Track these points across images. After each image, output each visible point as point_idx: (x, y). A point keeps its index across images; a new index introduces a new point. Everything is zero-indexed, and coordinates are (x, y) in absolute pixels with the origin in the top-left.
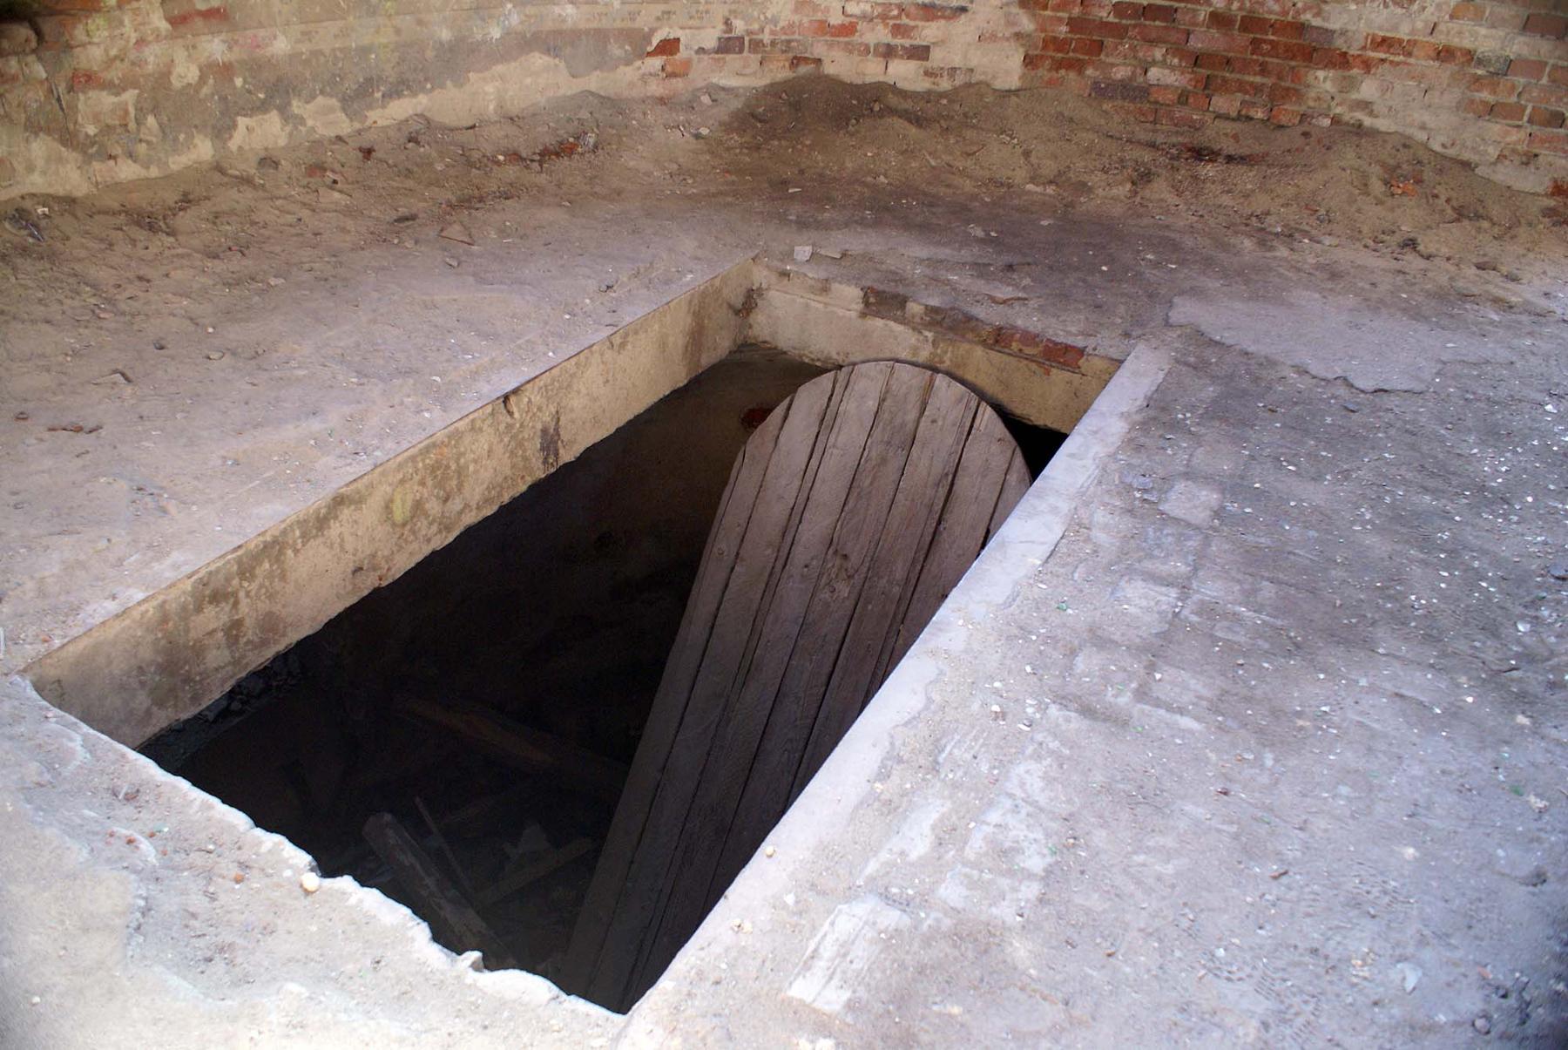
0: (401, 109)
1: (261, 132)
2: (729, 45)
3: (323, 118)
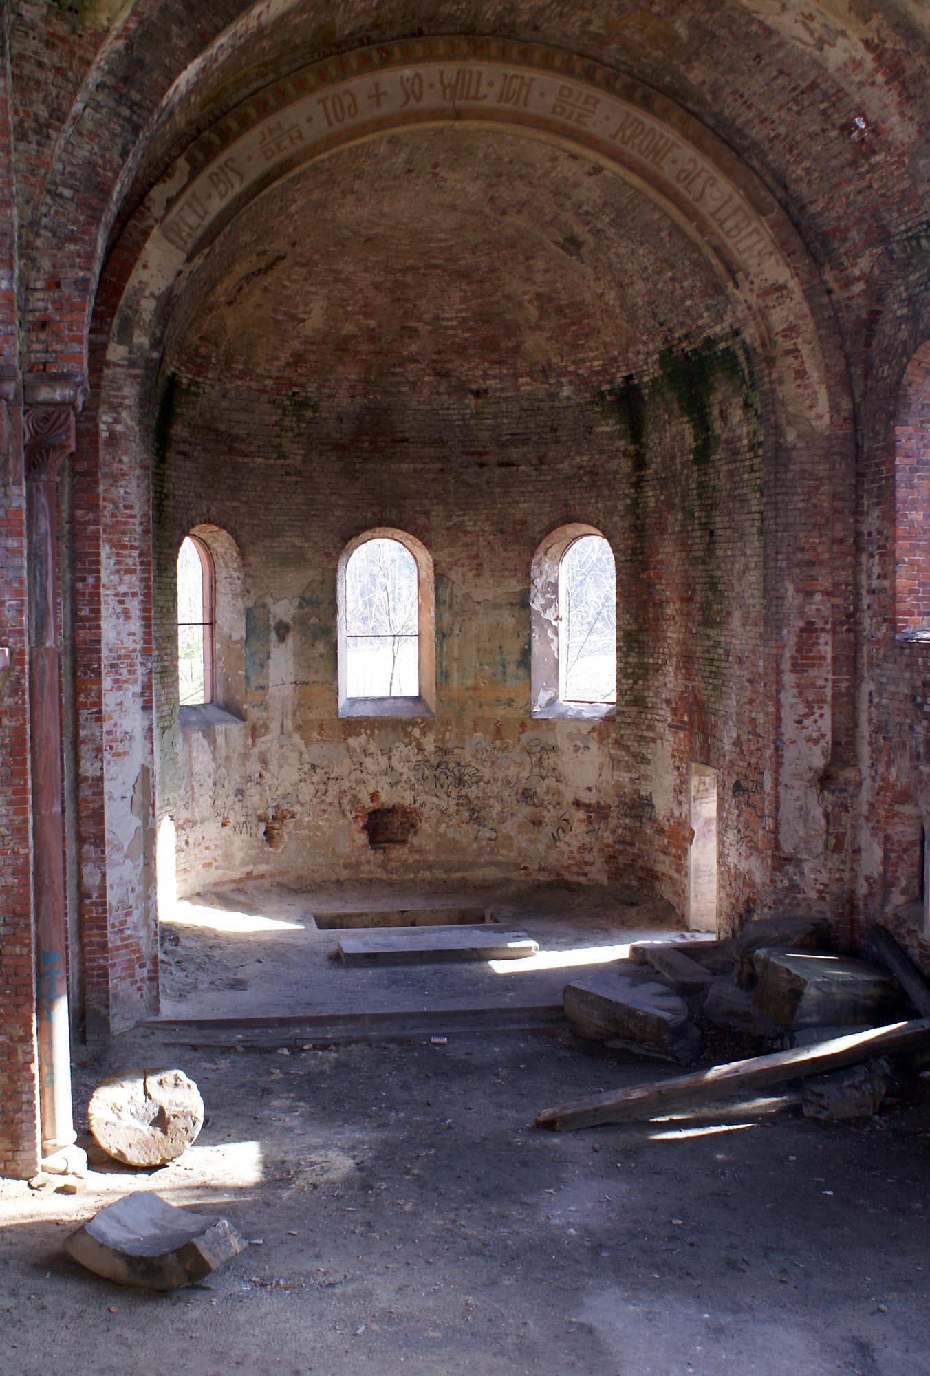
0: (459, 875)
1: (427, 874)
2: (541, 869)
3: (440, 874)
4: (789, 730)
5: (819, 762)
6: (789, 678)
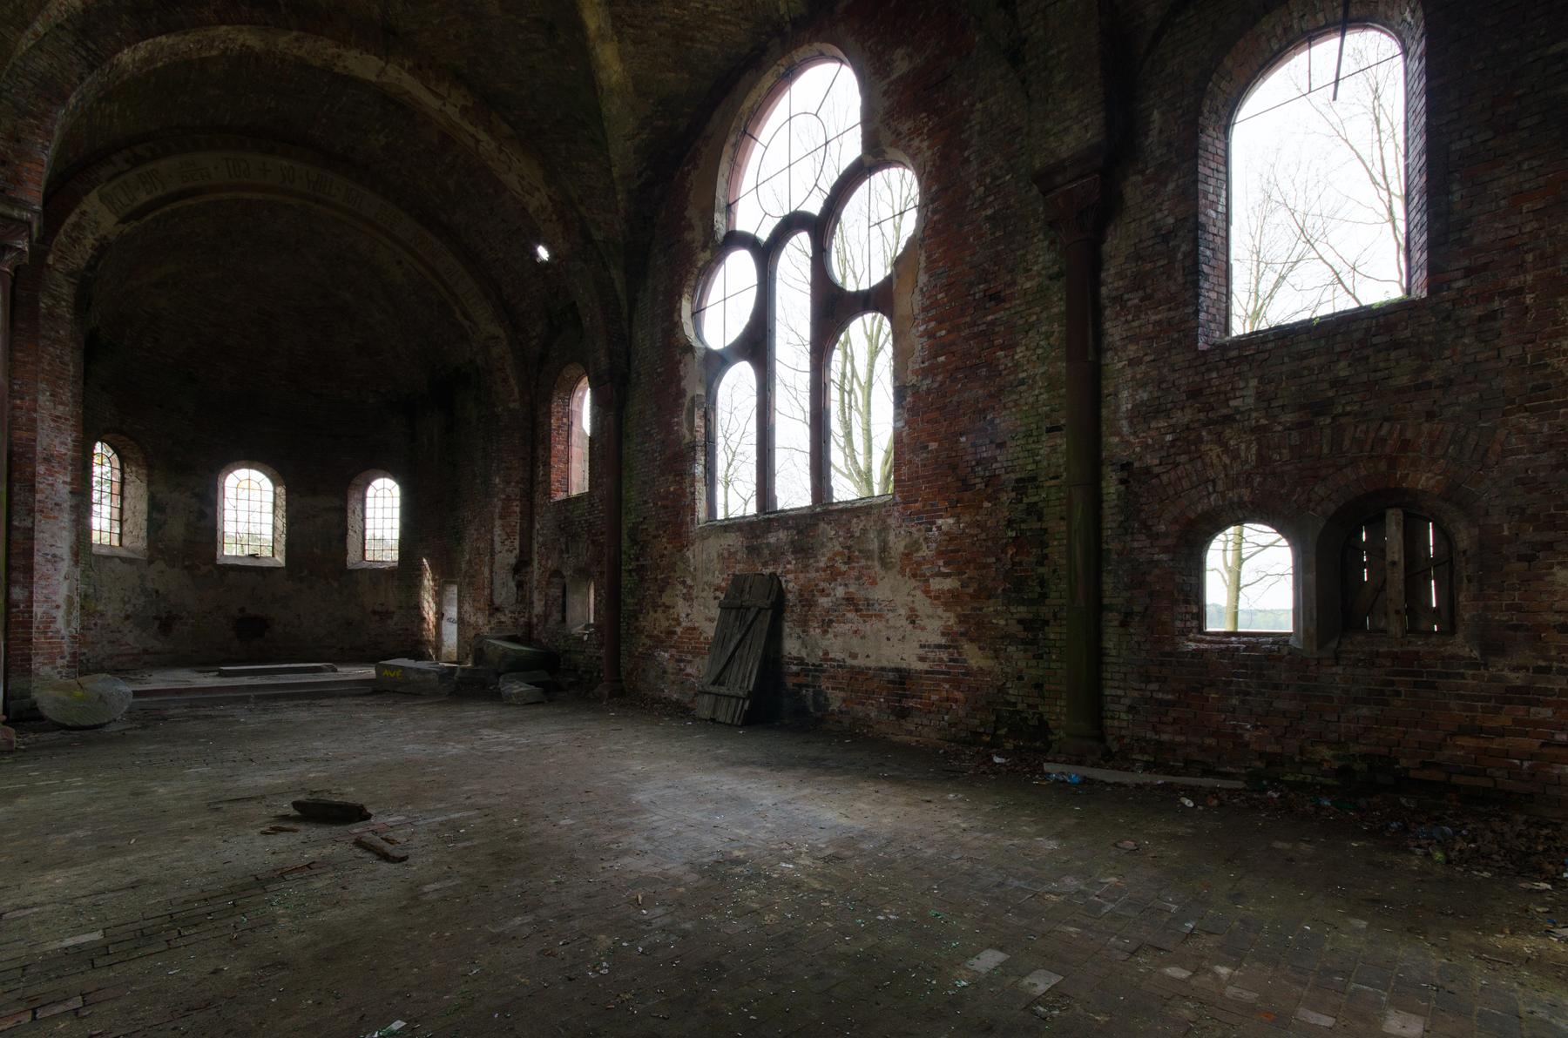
4: (498, 546)
5: (513, 561)
6: (498, 523)
